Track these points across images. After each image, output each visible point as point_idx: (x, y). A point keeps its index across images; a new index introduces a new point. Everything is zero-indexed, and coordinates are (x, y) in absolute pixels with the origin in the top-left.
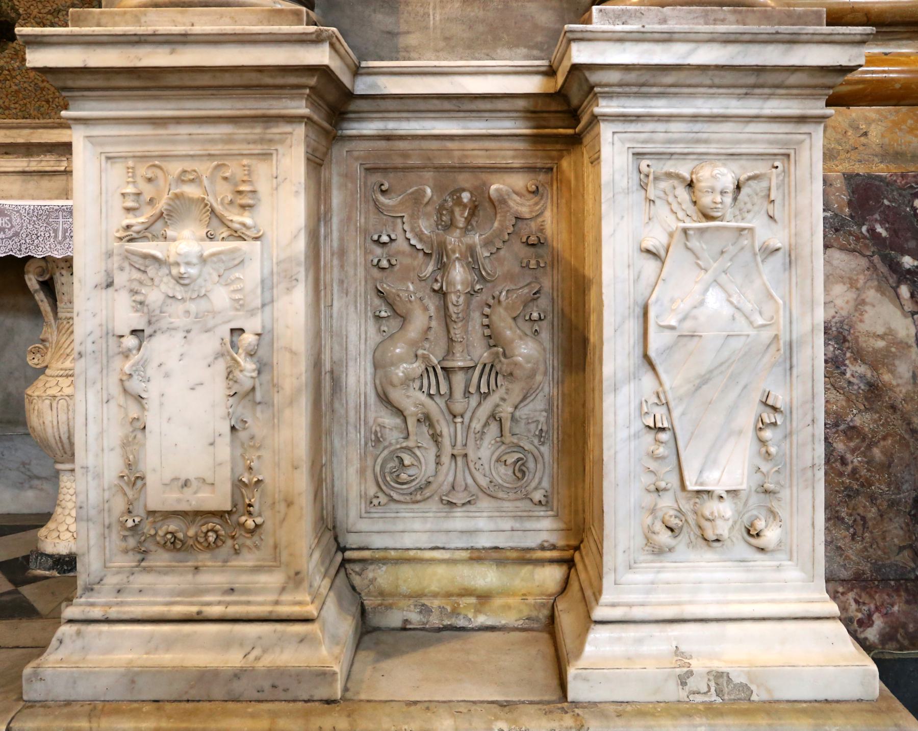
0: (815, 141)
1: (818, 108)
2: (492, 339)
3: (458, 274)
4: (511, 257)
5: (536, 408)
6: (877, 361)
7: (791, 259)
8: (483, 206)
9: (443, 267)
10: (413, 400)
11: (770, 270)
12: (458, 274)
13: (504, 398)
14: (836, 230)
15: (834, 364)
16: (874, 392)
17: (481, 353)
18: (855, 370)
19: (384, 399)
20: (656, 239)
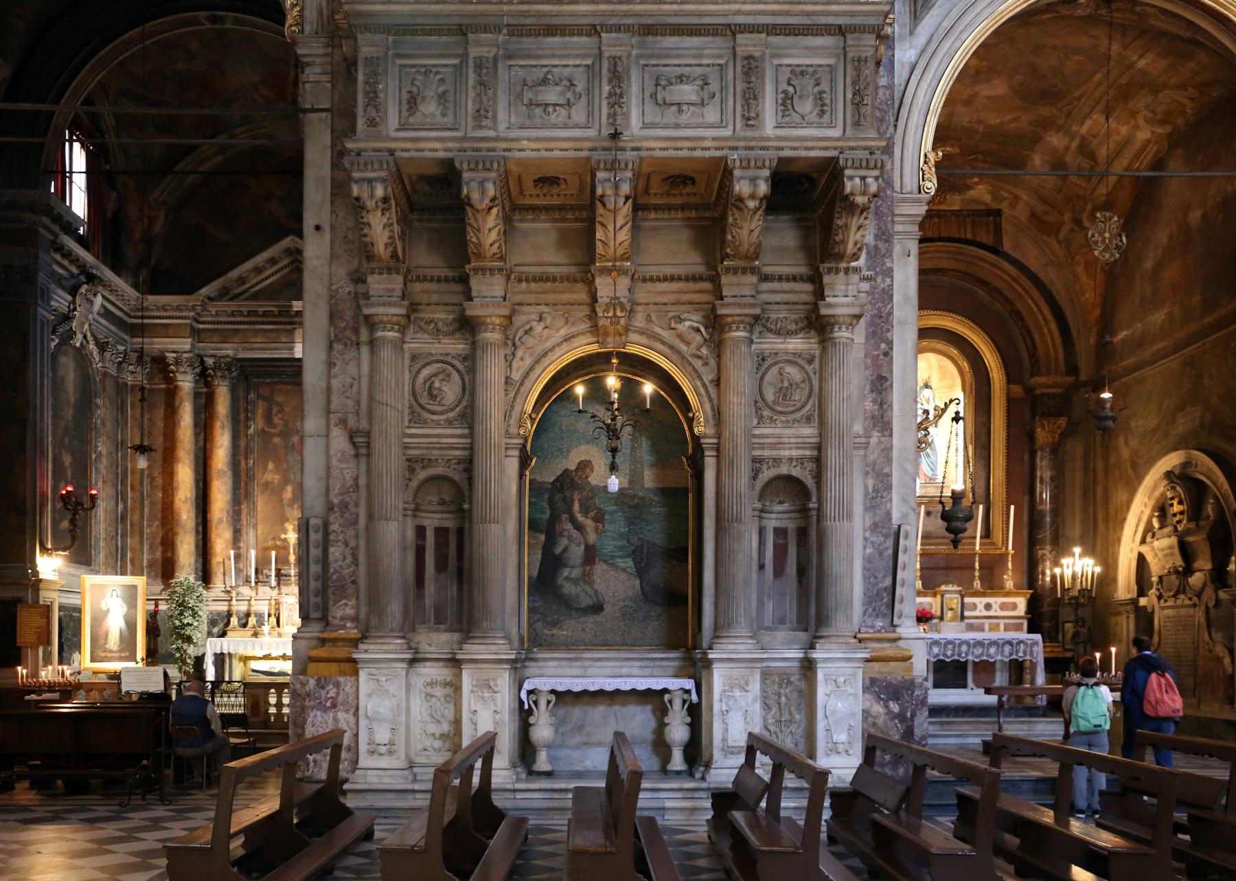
0: (861, 671)
1: (861, 665)
2: (790, 714)
3: (783, 699)
4: (795, 695)
5: (800, 730)
6: (875, 718)
7: (856, 695)
8: (790, 683)
9: (780, 697)
10: (772, 728)
11: (851, 698)
12: (783, 699)
13: (793, 728)
14: (866, 690)
15: (865, 719)
16: (874, 724)
17: (788, 717)
18: (870, 720)
19: (766, 728)
20: (828, 692)
